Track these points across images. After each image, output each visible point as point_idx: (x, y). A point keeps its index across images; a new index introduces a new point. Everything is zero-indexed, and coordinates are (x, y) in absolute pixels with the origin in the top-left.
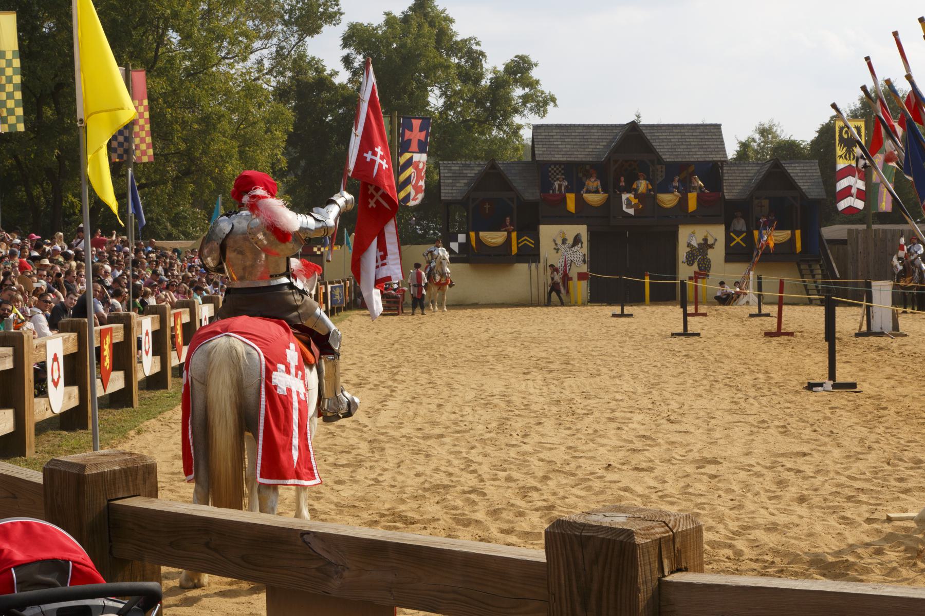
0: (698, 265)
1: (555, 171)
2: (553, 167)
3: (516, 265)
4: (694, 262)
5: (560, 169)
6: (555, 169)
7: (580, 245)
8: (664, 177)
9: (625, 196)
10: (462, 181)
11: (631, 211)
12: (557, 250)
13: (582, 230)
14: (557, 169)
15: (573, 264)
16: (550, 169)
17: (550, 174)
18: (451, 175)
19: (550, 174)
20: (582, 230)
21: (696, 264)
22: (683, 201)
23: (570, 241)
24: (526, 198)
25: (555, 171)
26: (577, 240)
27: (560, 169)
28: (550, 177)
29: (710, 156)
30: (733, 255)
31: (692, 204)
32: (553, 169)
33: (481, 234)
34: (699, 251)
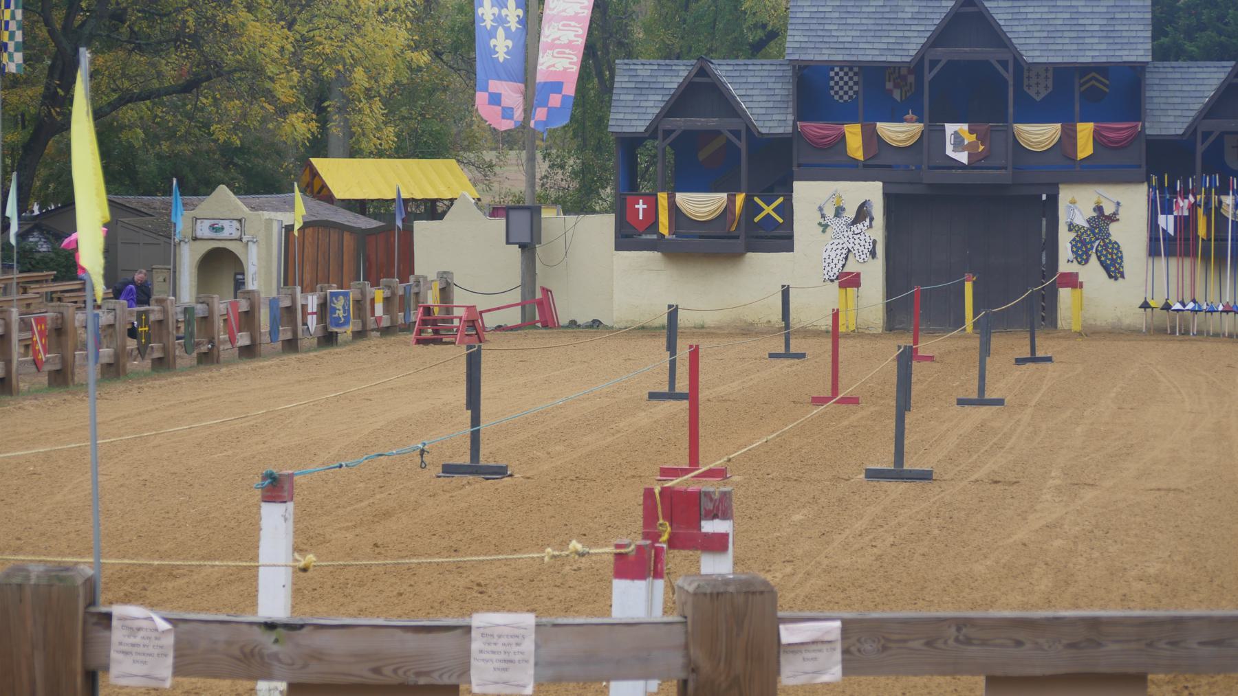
0: (1099, 258)
1: (841, 79)
2: (837, 69)
3: (749, 255)
4: (1089, 256)
5: (851, 74)
6: (841, 74)
7: (867, 223)
8: (1050, 90)
9: (950, 128)
10: (651, 98)
11: (963, 157)
12: (825, 227)
13: (872, 192)
14: (846, 74)
15: (851, 256)
16: (832, 74)
17: (832, 83)
18: (632, 85)
19: (832, 83)
20: (872, 192)
21: (1094, 259)
22: (1069, 137)
23: (851, 213)
24: (763, 131)
25: (841, 79)
26: (863, 213)
27: (851, 74)
28: (832, 88)
29: (1118, 53)
30: (1157, 244)
31: (1085, 147)
32: (837, 74)
33: (680, 197)
34: (1093, 232)
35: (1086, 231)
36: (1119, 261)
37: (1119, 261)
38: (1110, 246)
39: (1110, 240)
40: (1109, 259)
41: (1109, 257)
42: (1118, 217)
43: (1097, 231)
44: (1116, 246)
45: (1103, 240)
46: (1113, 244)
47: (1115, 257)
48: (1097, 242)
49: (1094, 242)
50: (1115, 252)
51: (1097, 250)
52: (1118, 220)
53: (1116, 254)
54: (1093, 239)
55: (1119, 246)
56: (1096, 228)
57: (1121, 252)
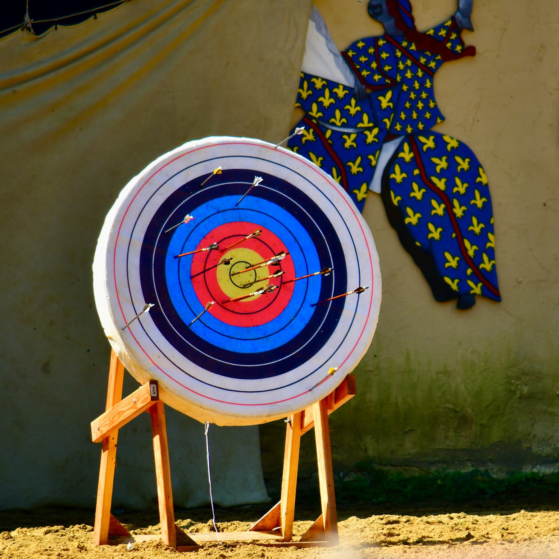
35: (340, 103)
36: (477, 228)
37: (477, 228)
38: (442, 164)
39: (439, 139)
40: (437, 221)
41: (439, 210)
42: (469, 39)
43: (385, 102)
44: (464, 164)
45: (415, 146)
46: (451, 156)
47: (459, 211)
48: (388, 150)
49: (377, 147)
50: (461, 188)
51: (387, 181)
52: (470, 51)
53: (465, 199)
54: (370, 138)
55: (475, 165)
56: (381, 89)
57: (485, 190)
